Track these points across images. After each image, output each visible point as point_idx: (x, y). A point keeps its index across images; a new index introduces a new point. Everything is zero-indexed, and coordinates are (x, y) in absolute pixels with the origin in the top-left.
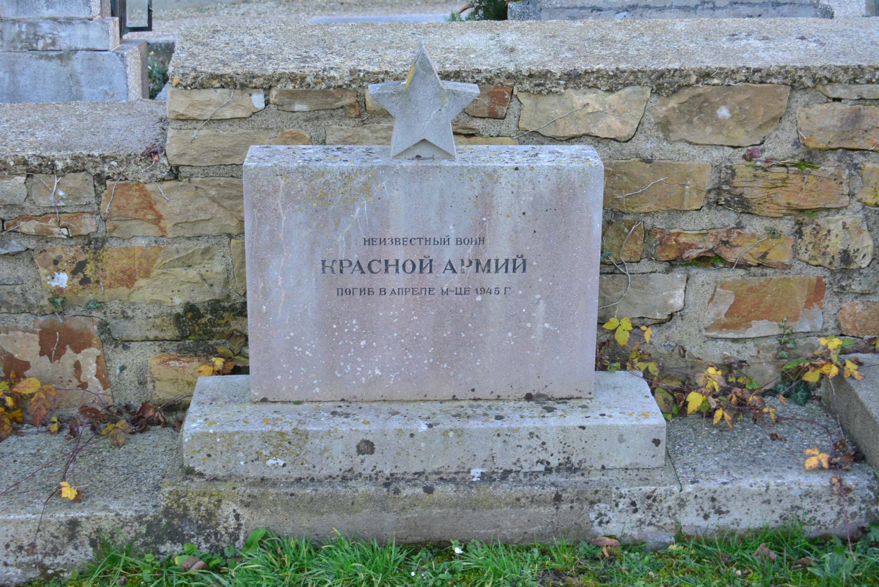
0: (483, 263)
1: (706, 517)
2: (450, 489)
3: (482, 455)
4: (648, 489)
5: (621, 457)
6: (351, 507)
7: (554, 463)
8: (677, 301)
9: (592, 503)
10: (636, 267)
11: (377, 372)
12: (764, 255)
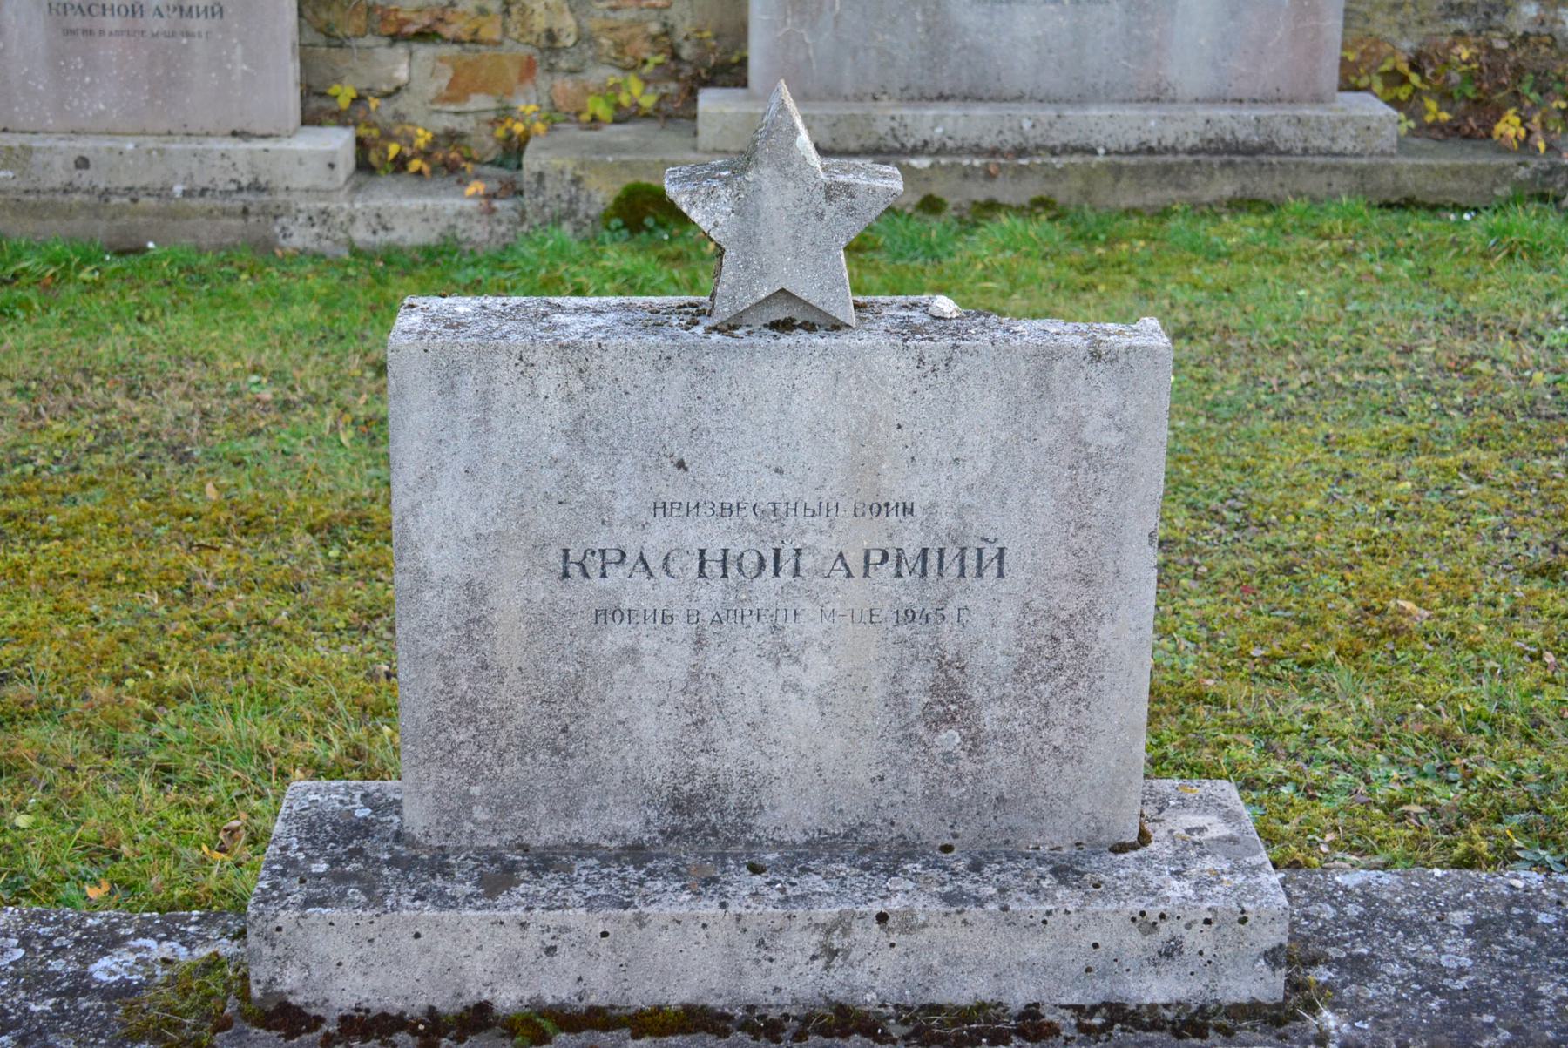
0: (186, 9)
1: (374, 232)
2: (153, 201)
3: (182, 173)
4: (322, 205)
5: (303, 179)
6: (68, 213)
7: (245, 182)
8: (402, 74)
9: (276, 217)
10: (361, 42)
11: (102, 107)
12: (476, 32)
